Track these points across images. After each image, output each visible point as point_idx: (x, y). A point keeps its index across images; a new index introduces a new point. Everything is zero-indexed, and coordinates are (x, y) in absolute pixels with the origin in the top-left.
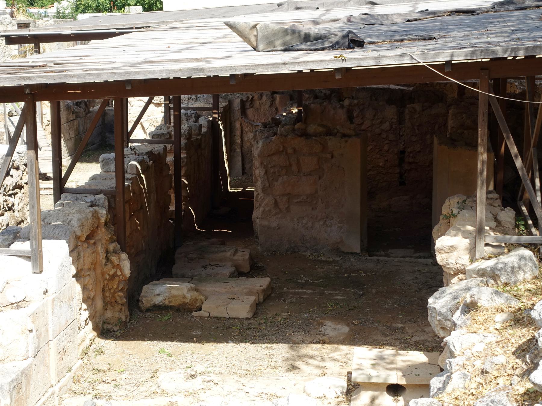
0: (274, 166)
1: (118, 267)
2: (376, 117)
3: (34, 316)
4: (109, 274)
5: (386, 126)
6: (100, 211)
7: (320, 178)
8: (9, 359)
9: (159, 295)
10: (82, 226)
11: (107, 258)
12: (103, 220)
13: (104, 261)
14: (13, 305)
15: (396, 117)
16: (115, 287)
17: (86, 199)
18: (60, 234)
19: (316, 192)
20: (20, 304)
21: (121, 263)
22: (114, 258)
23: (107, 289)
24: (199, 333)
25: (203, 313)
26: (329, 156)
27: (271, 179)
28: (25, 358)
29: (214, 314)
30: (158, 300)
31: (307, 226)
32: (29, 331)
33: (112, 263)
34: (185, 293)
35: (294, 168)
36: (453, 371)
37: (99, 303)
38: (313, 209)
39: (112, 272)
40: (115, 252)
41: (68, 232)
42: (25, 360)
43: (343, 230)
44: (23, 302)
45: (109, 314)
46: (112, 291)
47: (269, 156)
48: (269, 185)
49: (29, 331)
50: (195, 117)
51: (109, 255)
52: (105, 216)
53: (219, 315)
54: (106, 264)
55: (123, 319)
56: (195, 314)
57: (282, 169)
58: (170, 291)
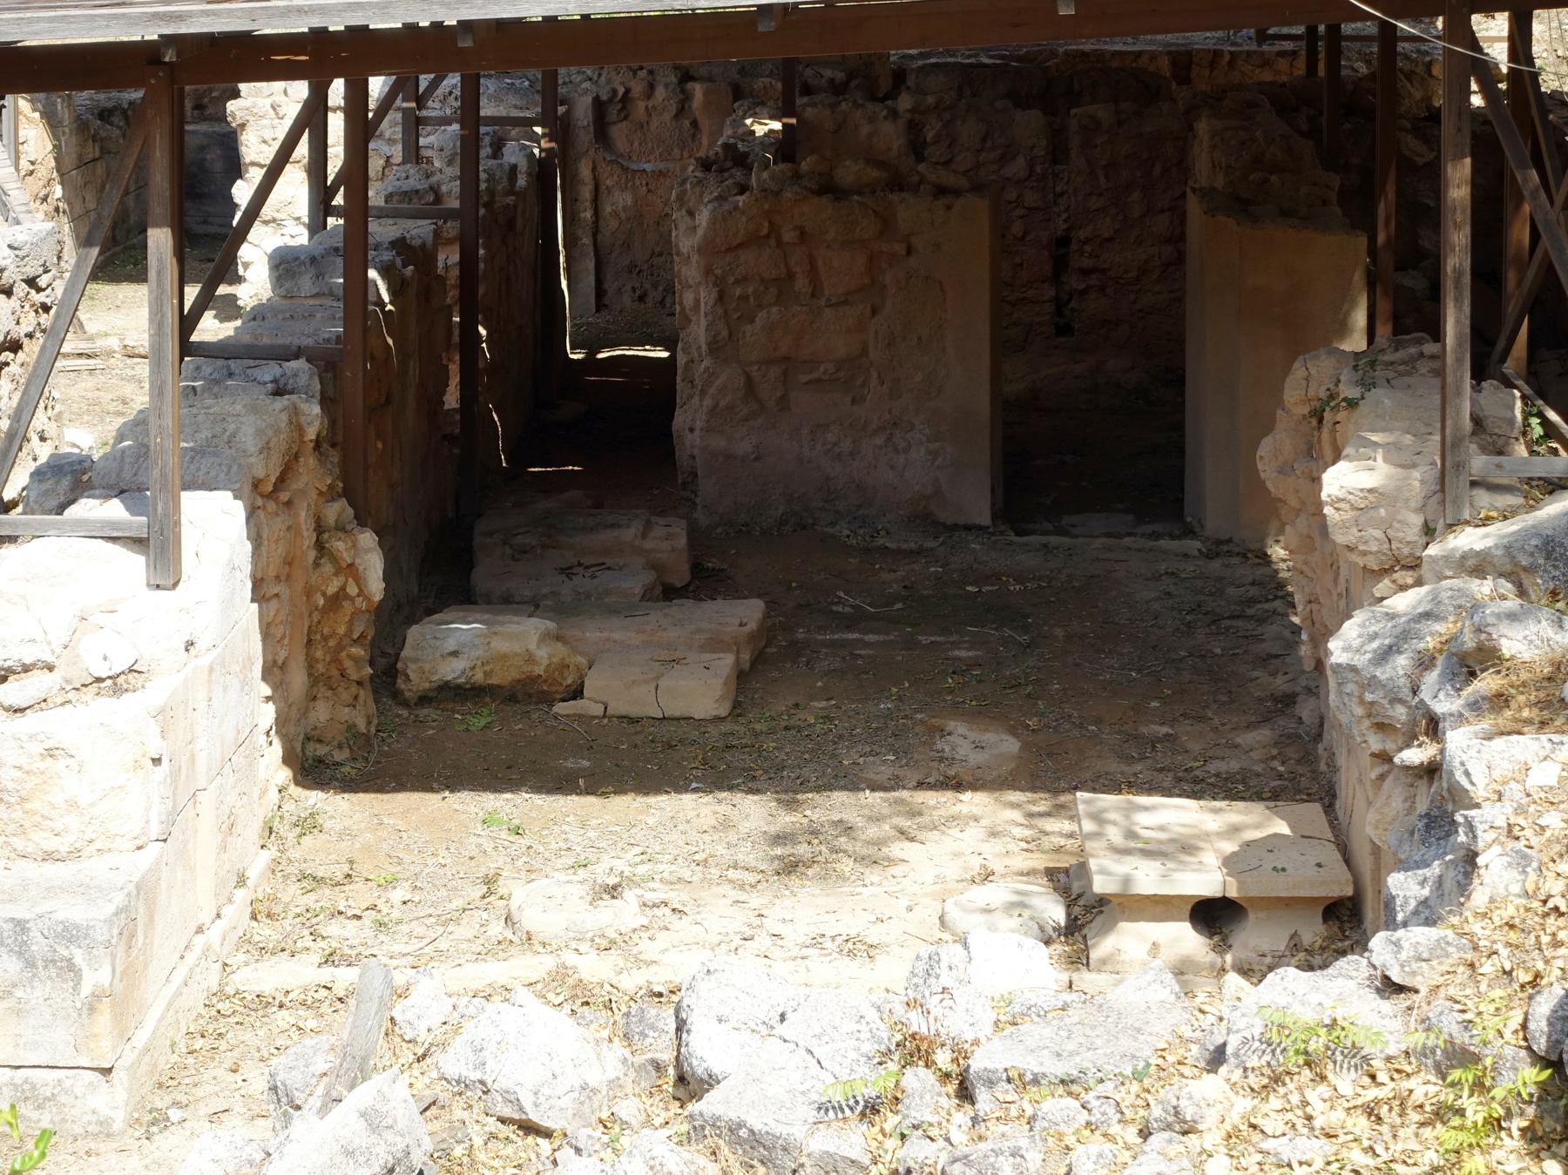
0: (744, 280)
1: (351, 570)
2: (989, 144)
3: (164, 716)
4: (324, 594)
5: (1017, 167)
6: (304, 407)
7: (874, 312)
8: (93, 847)
9: (455, 654)
10: (266, 449)
11: (320, 546)
12: (311, 434)
13: (312, 554)
14: (103, 685)
15: (1044, 143)
16: (342, 630)
17: (257, 373)
18: (213, 473)
19: (864, 351)
20: (121, 680)
21: (358, 561)
22: (339, 545)
23: (318, 637)
24: (586, 763)
25: (587, 707)
26: (900, 248)
27: (735, 316)
28: (139, 843)
29: (619, 707)
30: (452, 671)
31: (837, 450)
32: (153, 760)
33: (334, 559)
34: (532, 647)
35: (801, 283)
36: (1481, 844)
37: (298, 679)
38: (854, 401)
39: (332, 588)
40: (341, 528)
41: (235, 468)
42: (139, 848)
43: (940, 459)
44: (130, 676)
45: (321, 713)
46: (332, 643)
47: (728, 250)
48: (730, 334)
49: (153, 760)
50: (491, 145)
51: (326, 536)
52: (317, 424)
53: (634, 711)
54: (316, 564)
55: (362, 726)
56: (561, 708)
57: (766, 288)
58: (489, 643)
